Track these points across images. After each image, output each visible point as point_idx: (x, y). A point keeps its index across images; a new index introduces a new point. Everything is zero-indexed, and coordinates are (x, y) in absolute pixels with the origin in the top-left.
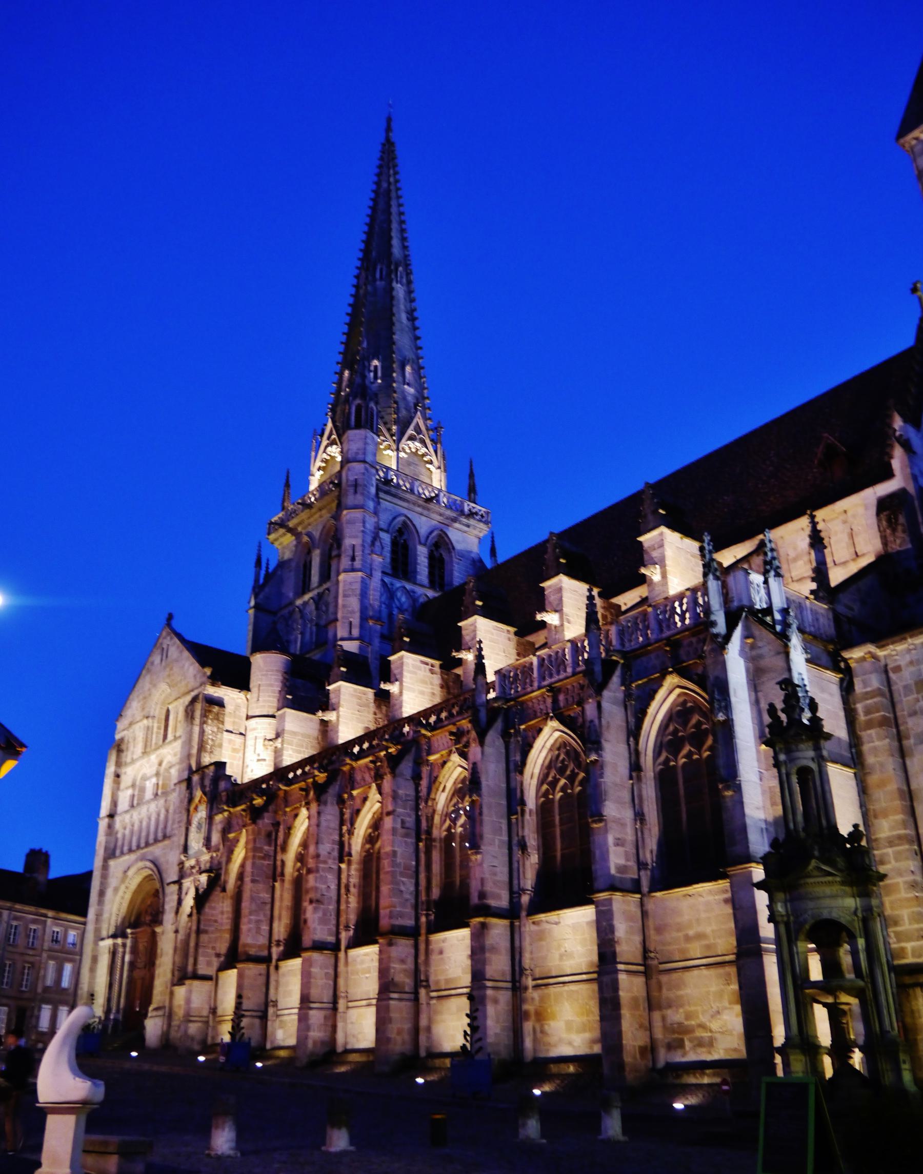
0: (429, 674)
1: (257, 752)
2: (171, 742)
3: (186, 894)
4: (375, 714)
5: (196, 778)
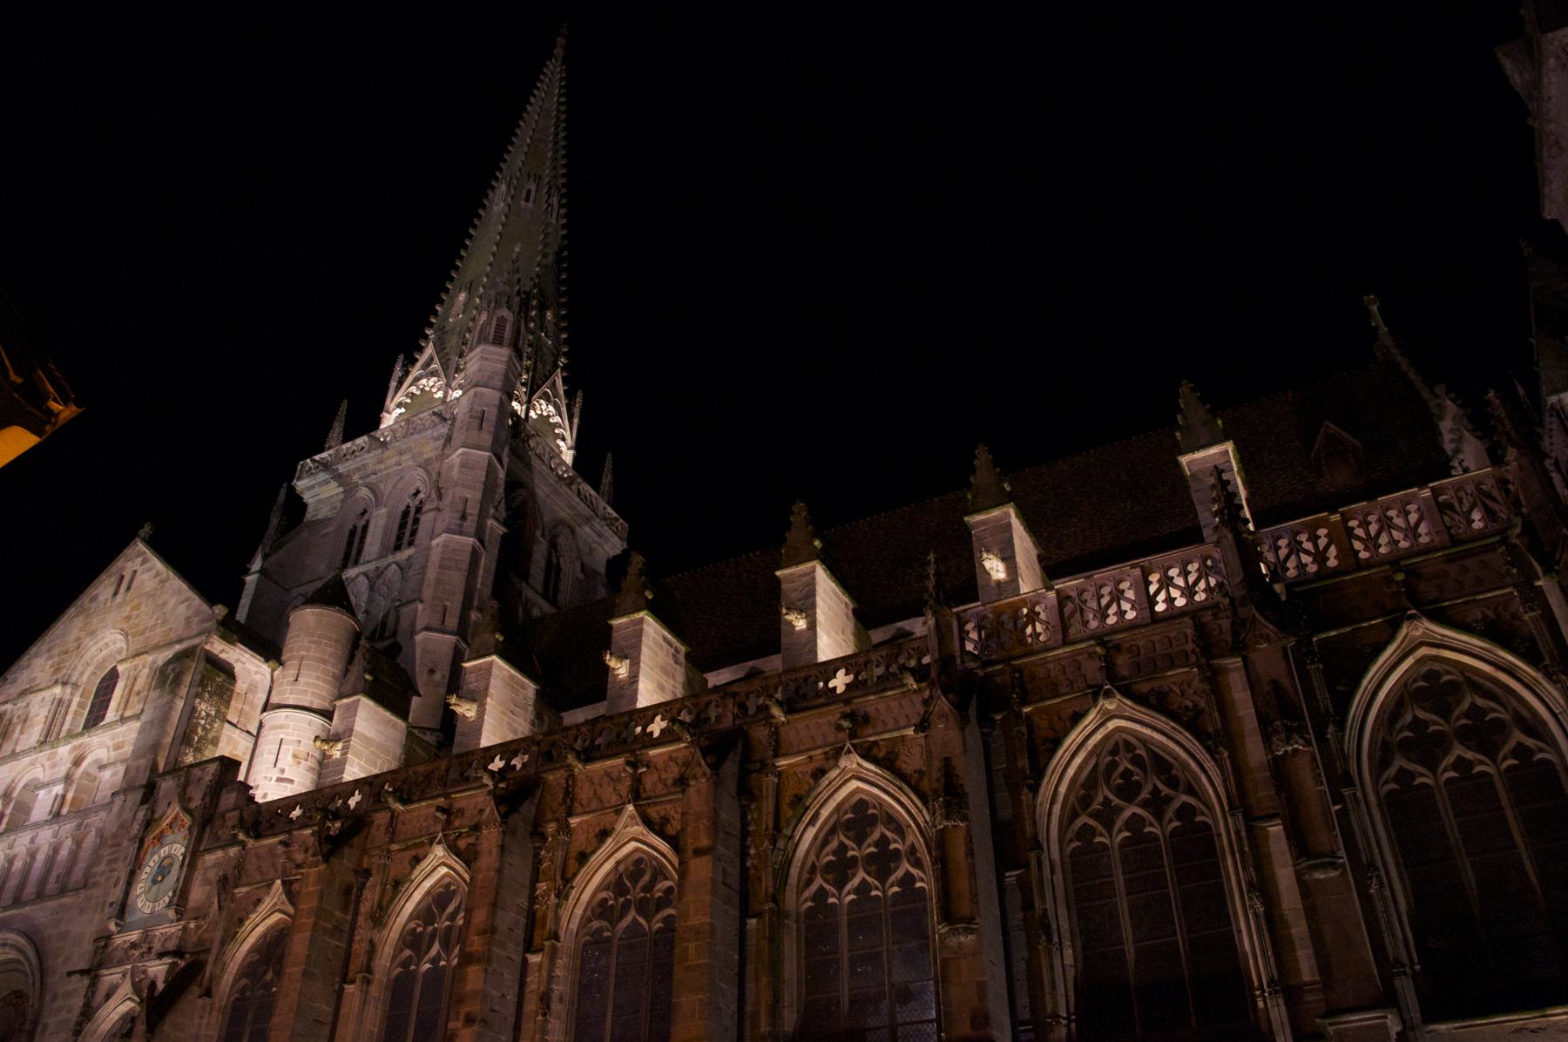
0: (672, 662)
1: (278, 765)
2: (111, 725)
3: (108, 997)
5: (167, 785)
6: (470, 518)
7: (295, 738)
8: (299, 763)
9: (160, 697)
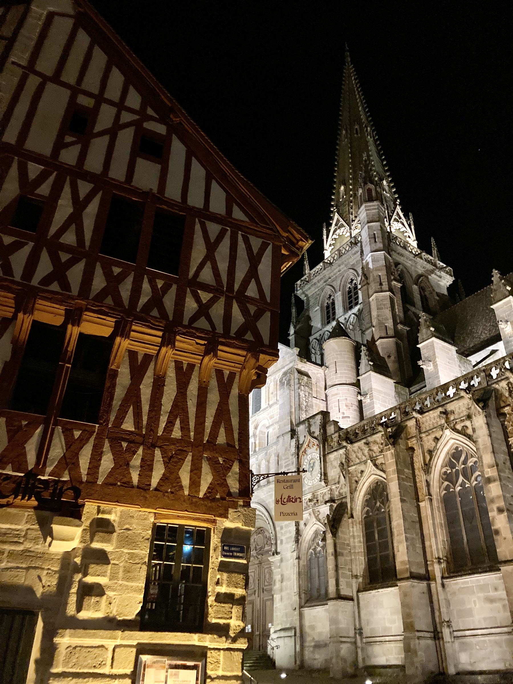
3: (305, 524)
4: (460, 367)
5: (301, 430)
6: (384, 284)
7: (344, 398)
8: (349, 408)
9: (284, 392)
